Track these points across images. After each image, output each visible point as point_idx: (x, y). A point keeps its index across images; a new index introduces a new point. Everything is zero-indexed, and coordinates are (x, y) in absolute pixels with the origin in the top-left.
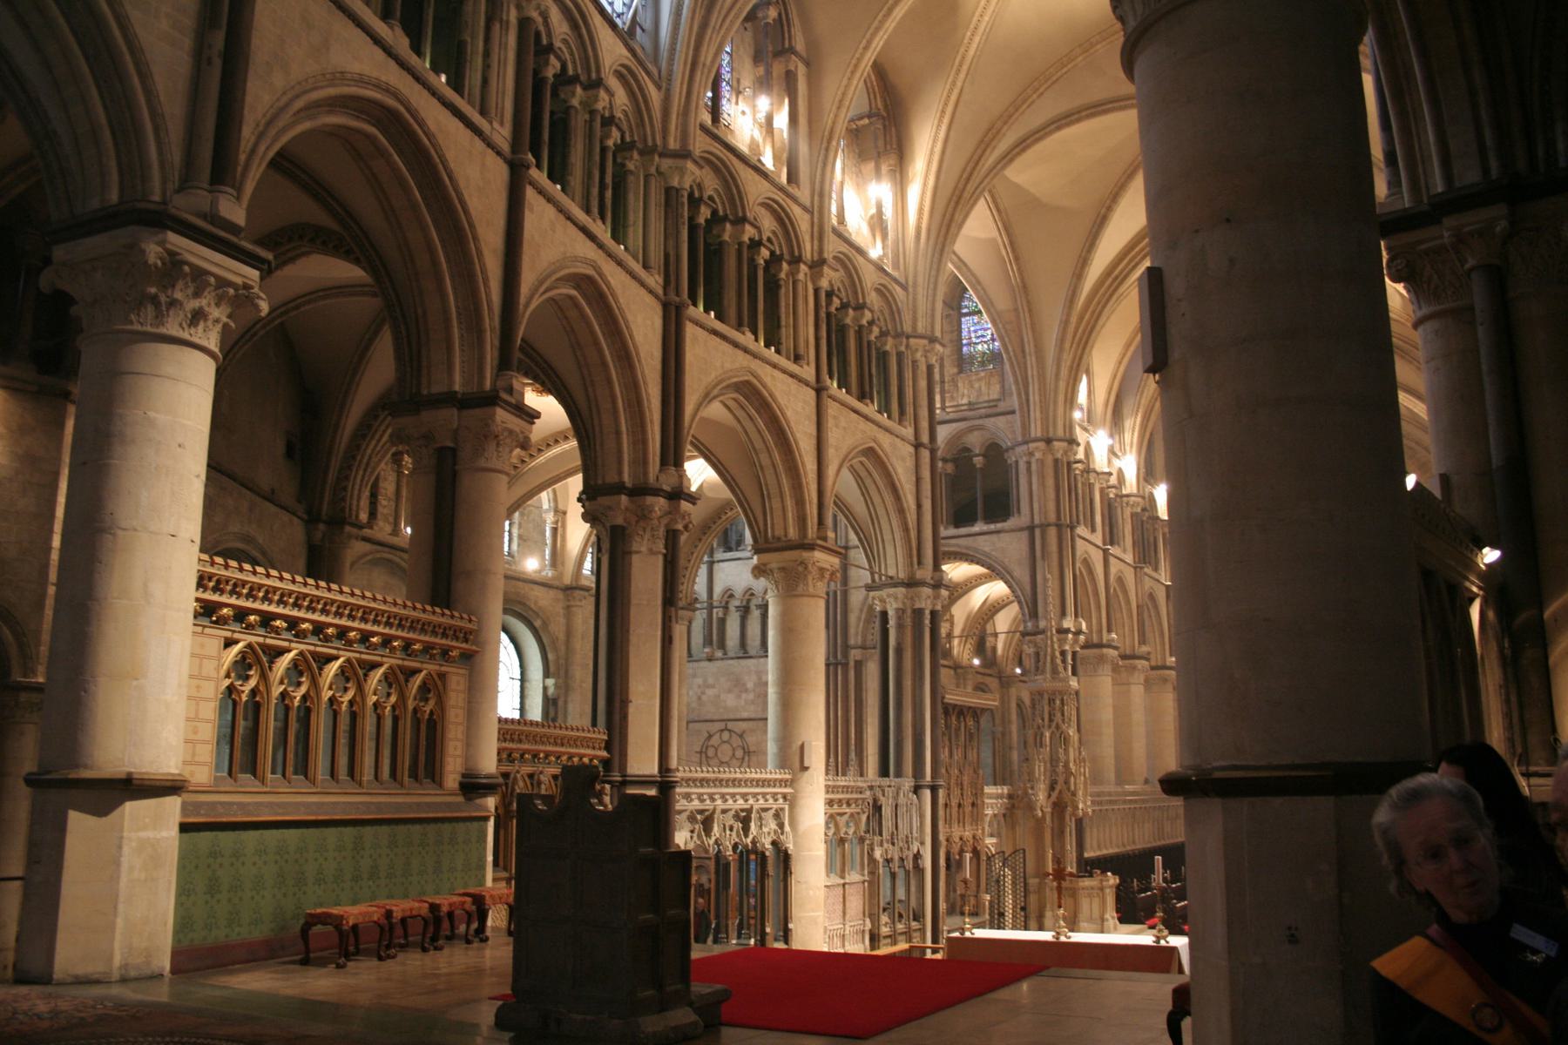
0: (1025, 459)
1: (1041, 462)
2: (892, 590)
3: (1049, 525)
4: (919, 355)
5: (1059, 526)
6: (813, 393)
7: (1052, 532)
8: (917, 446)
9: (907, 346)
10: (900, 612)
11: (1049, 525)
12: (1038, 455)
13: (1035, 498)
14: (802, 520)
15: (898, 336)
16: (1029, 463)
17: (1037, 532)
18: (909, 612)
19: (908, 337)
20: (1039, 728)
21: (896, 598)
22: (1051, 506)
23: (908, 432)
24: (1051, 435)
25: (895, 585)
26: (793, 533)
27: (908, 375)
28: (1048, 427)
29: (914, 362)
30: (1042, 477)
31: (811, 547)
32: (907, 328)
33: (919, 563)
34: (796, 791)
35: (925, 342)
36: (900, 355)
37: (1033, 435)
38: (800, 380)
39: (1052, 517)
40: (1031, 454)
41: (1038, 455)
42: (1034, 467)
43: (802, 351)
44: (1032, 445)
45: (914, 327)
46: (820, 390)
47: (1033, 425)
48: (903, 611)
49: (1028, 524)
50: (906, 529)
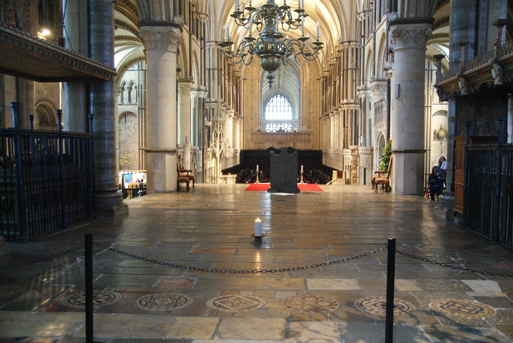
0: (208, 47)
1: (213, 49)
2: (193, 92)
3: (215, 69)
4: (202, 20)
5: (218, 70)
6: (189, 35)
7: (216, 71)
8: (201, 49)
9: (200, 17)
10: (195, 98)
11: (215, 69)
12: (213, 46)
13: (211, 60)
14: (186, 73)
15: (198, 13)
16: (209, 49)
17: (211, 71)
18: (197, 98)
19: (200, 14)
20: (216, 131)
21: (194, 94)
22: (216, 63)
23: (199, 44)
24: (217, 41)
25: (195, 90)
26: (184, 77)
27: (199, 26)
28: (216, 38)
29: (201, 22)
30: (213, 54)
31: (190, 82)
32: (200, 11)
33: (201, 84)
34: (185, 150)
35: (204, 16)
36: (197, 19)
37: (211, 40)
38: (187, 31)
39: (216, 67)
40: (210, 46)
41: (213, 46)
42: (211, 50)
43: (186, 22)
44: (211, 43)
45: (202, 11)
46: (190, 35)
47: (212, 36)
48: (196, 98)
49: (208, 68)
50: (198, 74)
